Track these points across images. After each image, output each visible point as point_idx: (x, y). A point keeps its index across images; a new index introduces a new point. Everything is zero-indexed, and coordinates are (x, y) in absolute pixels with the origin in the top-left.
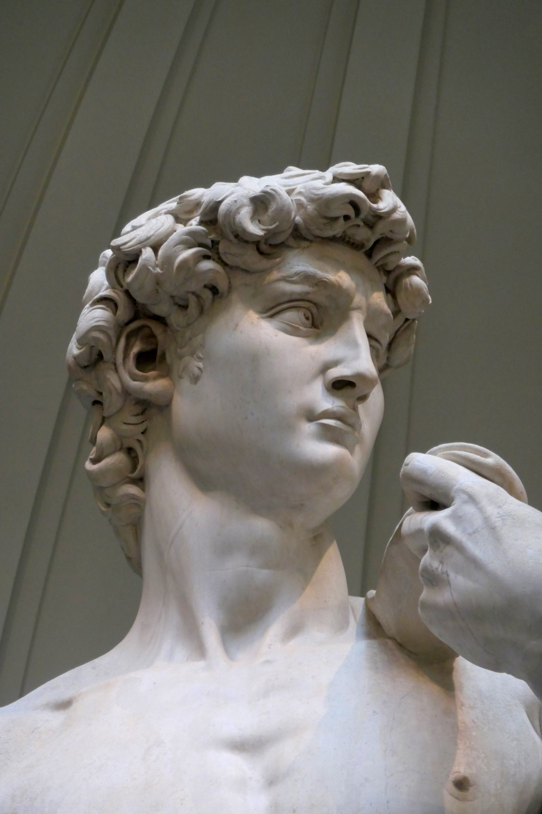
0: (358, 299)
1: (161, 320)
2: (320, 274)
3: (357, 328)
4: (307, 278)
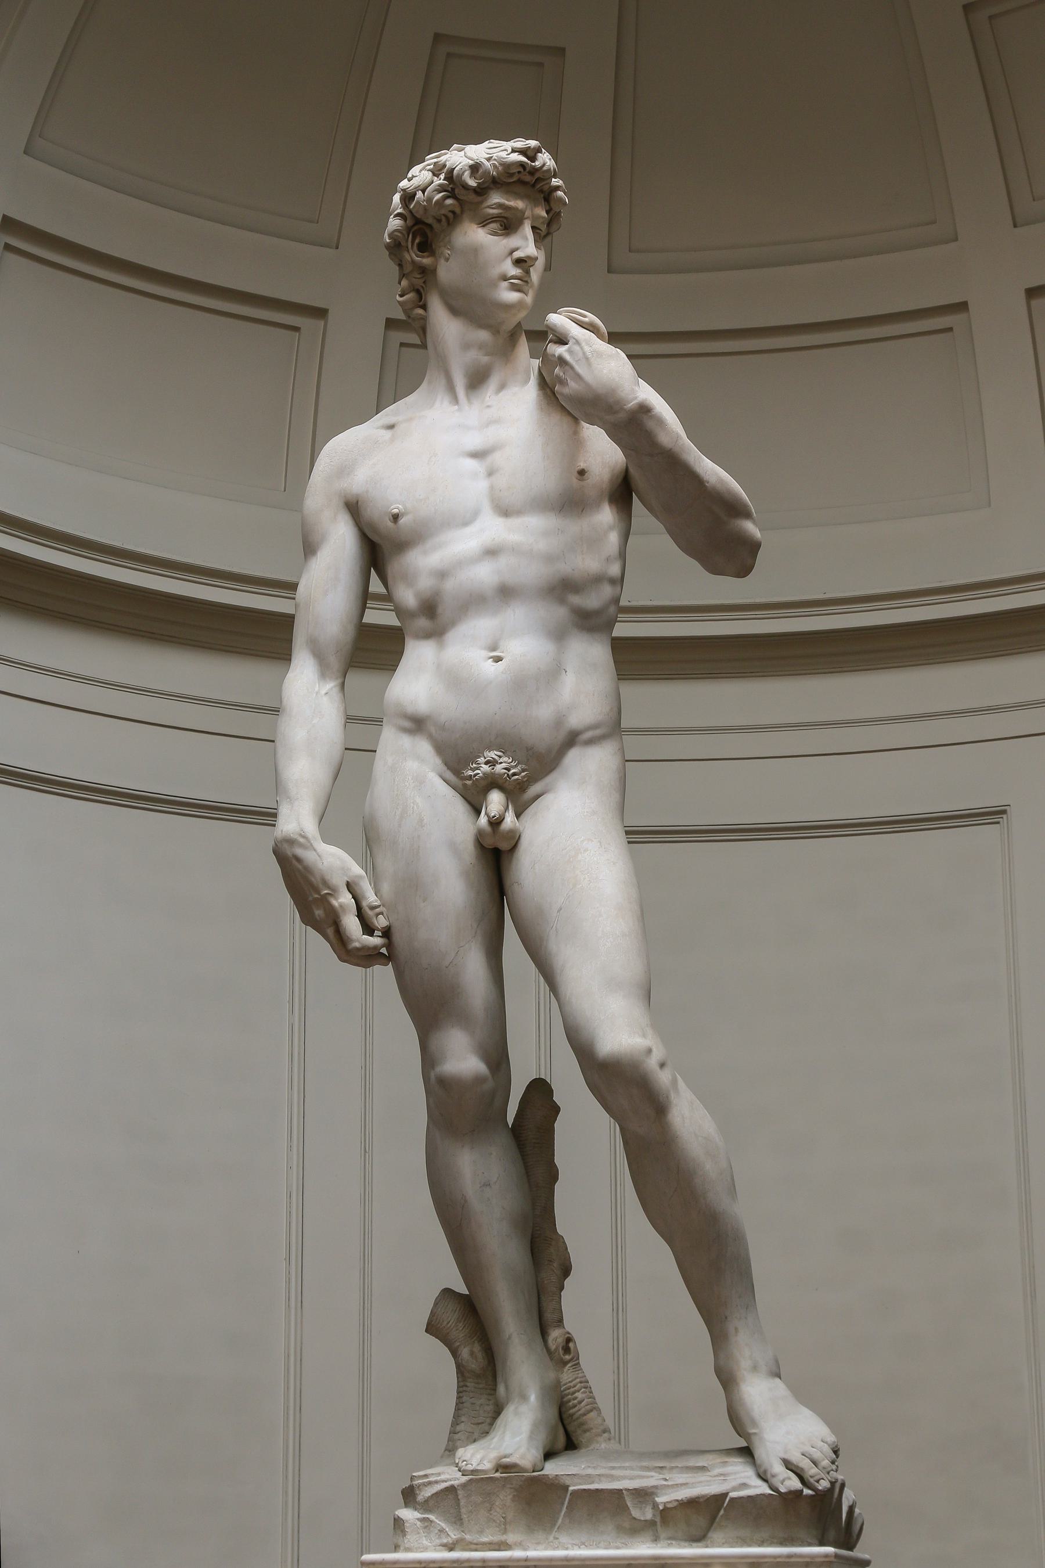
0: (528, 213)
1: (430, 226)
2: (507, 202)
3: (527, 229)
4: (500, 206)
